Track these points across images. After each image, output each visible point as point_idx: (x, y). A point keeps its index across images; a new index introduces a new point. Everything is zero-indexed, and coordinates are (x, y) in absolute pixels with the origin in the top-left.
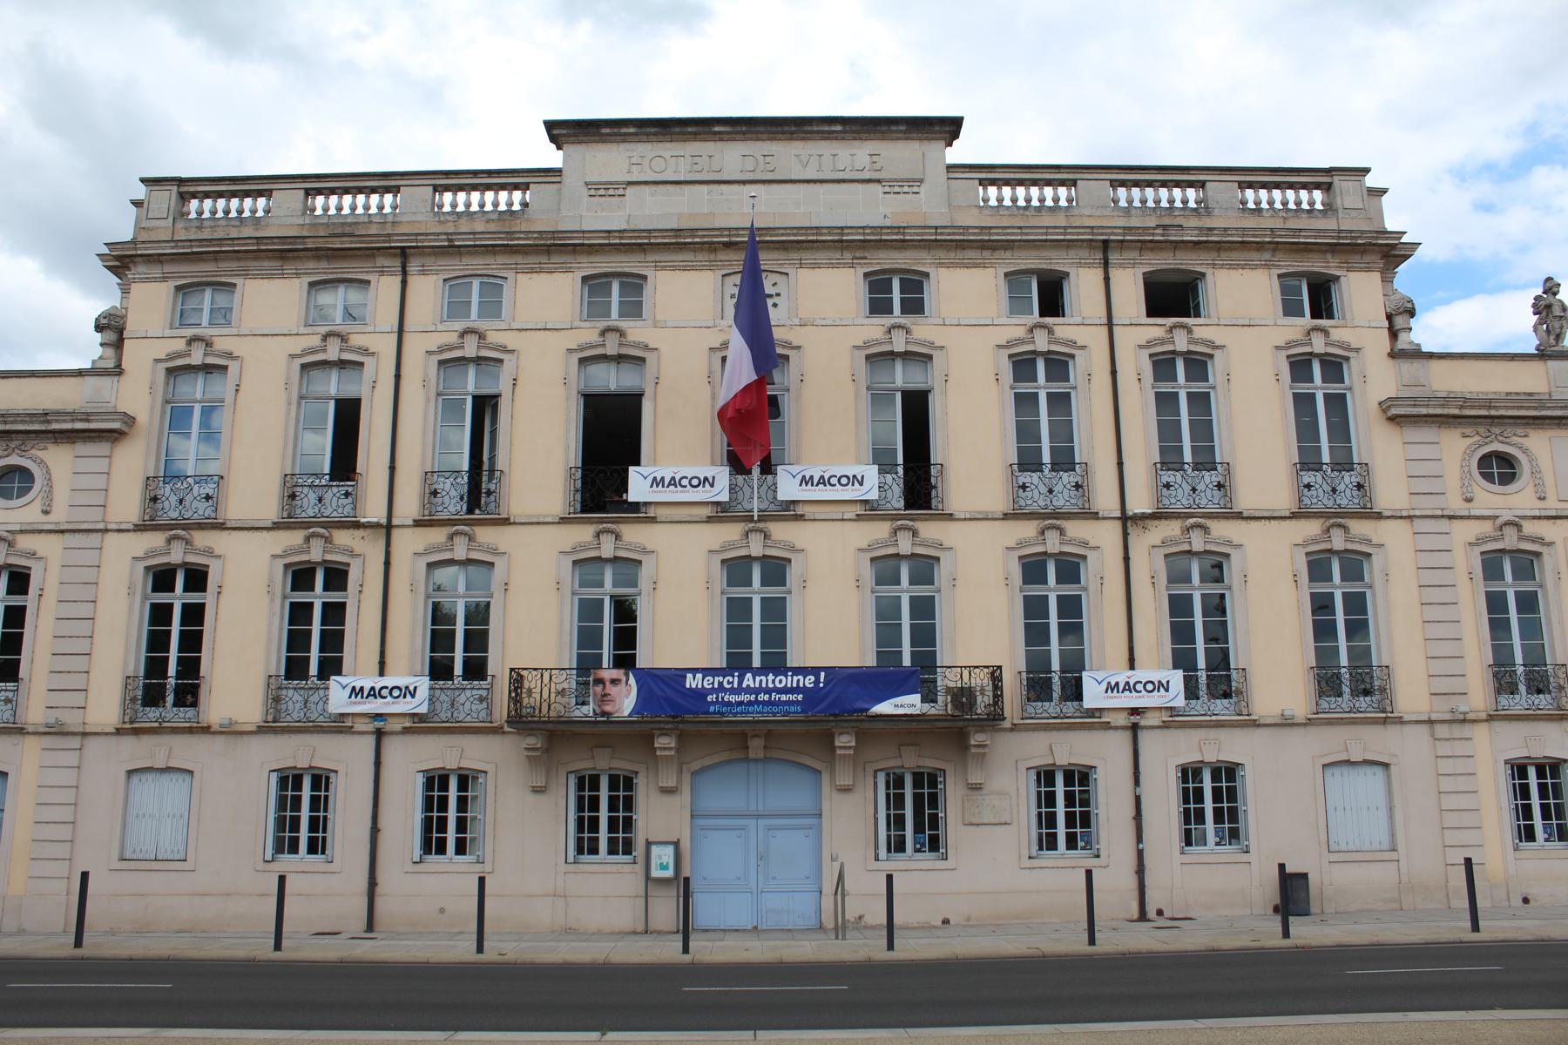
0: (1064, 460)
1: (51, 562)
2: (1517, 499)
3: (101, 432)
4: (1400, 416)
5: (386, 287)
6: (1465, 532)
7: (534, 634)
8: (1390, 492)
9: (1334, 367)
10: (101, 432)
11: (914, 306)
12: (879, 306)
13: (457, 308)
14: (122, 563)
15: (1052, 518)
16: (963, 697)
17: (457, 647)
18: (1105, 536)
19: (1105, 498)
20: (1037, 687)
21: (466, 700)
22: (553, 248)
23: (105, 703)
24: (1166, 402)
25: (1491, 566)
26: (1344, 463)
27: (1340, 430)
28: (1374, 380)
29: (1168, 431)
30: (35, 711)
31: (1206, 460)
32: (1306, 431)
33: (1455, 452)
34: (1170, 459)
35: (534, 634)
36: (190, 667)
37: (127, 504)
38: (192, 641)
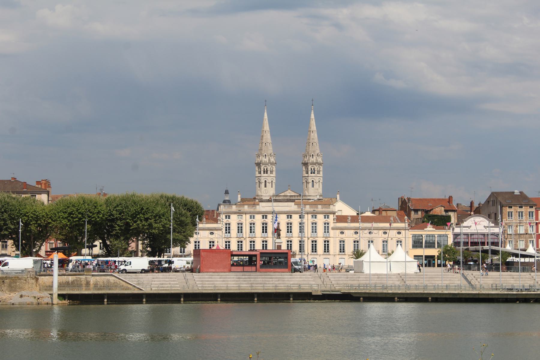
2: (343, 236)
4: (333, 229)
6: (338, 239)
8: (331, 235)
9: (328, 224)
12: (288, 218)
13: (251, 218)
16: (294, 252)
19: (306, 236)
22: (259, 213)
24: (313, 227)
25: (340, 242)
26: (328, 232)
27: (328, 229)
28: (331, 225)
29: (313, 229)
32: (325, 229)
33: (339, 231)
34: (313, 232)
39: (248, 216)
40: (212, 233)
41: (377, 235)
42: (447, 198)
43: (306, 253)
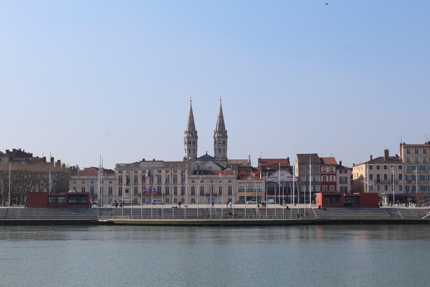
0: (168, 181)
1: (113, 187)
3: (115, 179)
5: (131, 171)
7: (140, 191)
10: (115, 179)
11: (161, 172)
13: (135, 172)
14: (118, 187)
15: (167, 184)
17: (136, 191)
18: (170, 186)
20: (166, 194)
21: (137, 194)
23: (117, 195)
30: (113, 195)
31: (176, 181)
35: (140, 191)
36: (122, 193)
37: (117, 184)
38: (122, 191)
39: (133, 171)
40: (111, 183)
41: (216, 183)
42: (287, 158)
43: (170, 195)
